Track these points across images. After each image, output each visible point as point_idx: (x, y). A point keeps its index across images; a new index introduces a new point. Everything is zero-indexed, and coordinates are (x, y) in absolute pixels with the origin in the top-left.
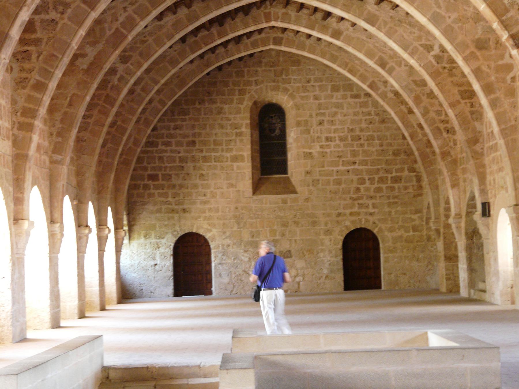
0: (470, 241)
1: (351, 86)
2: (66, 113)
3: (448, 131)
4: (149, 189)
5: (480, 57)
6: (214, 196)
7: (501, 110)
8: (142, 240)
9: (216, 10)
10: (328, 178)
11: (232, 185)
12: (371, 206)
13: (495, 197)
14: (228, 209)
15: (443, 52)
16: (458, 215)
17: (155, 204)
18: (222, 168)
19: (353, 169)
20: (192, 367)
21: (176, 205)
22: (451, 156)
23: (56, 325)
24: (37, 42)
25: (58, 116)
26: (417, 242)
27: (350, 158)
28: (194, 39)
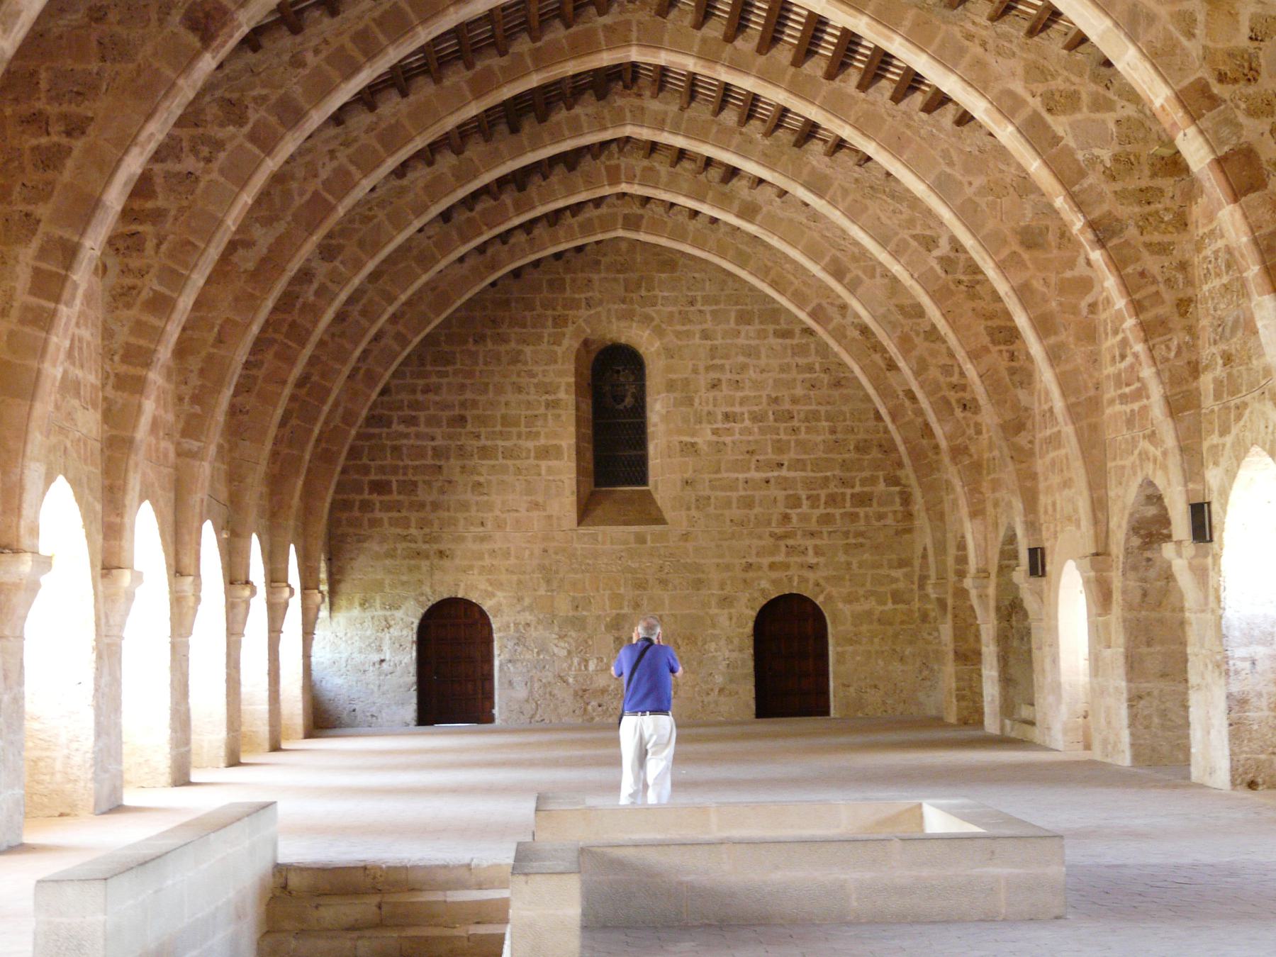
0: (1005, 624)
1: (775, 313)
2: (210, 357)
3: (965, 406)
4: (372, 511)
5: (1029, 264)
6: (500, 525)
7: (1068, 367)
8: (356, 612)
9: (512, 159)
10: (728, 494)
11: (537, 504)
12: (811, 552)
13: (1056, 538)
14: (527, 553)
15: (957, 251)
16: (983, 573)
17: (383, 540)
18: (519, 471)
19: (778, 477)
20: (456, 867)
21: (425, 542)
22: (971, 456)
23: (181, 779)
24: (157, 216)
25: (195, 363)
26: (902, 622)
27: (771, 456)
28: (468, 214)
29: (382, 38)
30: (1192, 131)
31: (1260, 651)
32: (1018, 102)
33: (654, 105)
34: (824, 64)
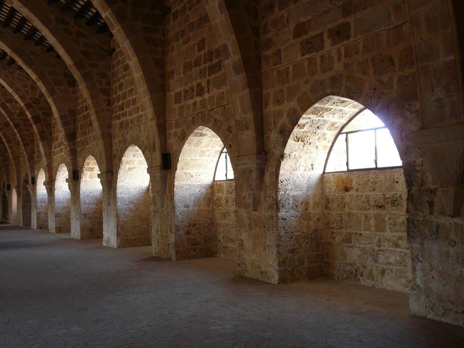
30: (28, 111)
31: (43, 204)
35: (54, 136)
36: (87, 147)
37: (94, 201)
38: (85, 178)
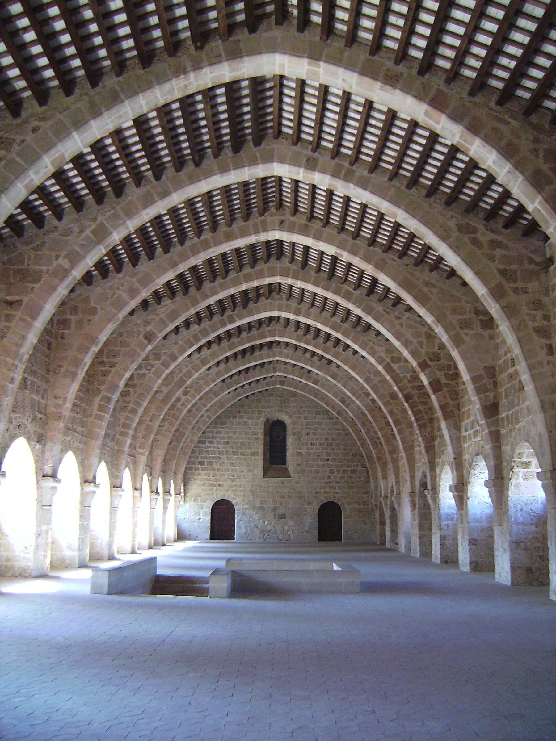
2: (148, 425)
8: (192, 502)
17: (202, 480)
24: (134, 386)
27: (325, 456)
29: (201, 337)
30: (422, 374)
31: (450, 523)
32: (384, 360)
33: (285, 351)
34: (332, 343)
35: (463, 410)
36: (517, 427)
37: (532, 520)
38: (516, 479)
